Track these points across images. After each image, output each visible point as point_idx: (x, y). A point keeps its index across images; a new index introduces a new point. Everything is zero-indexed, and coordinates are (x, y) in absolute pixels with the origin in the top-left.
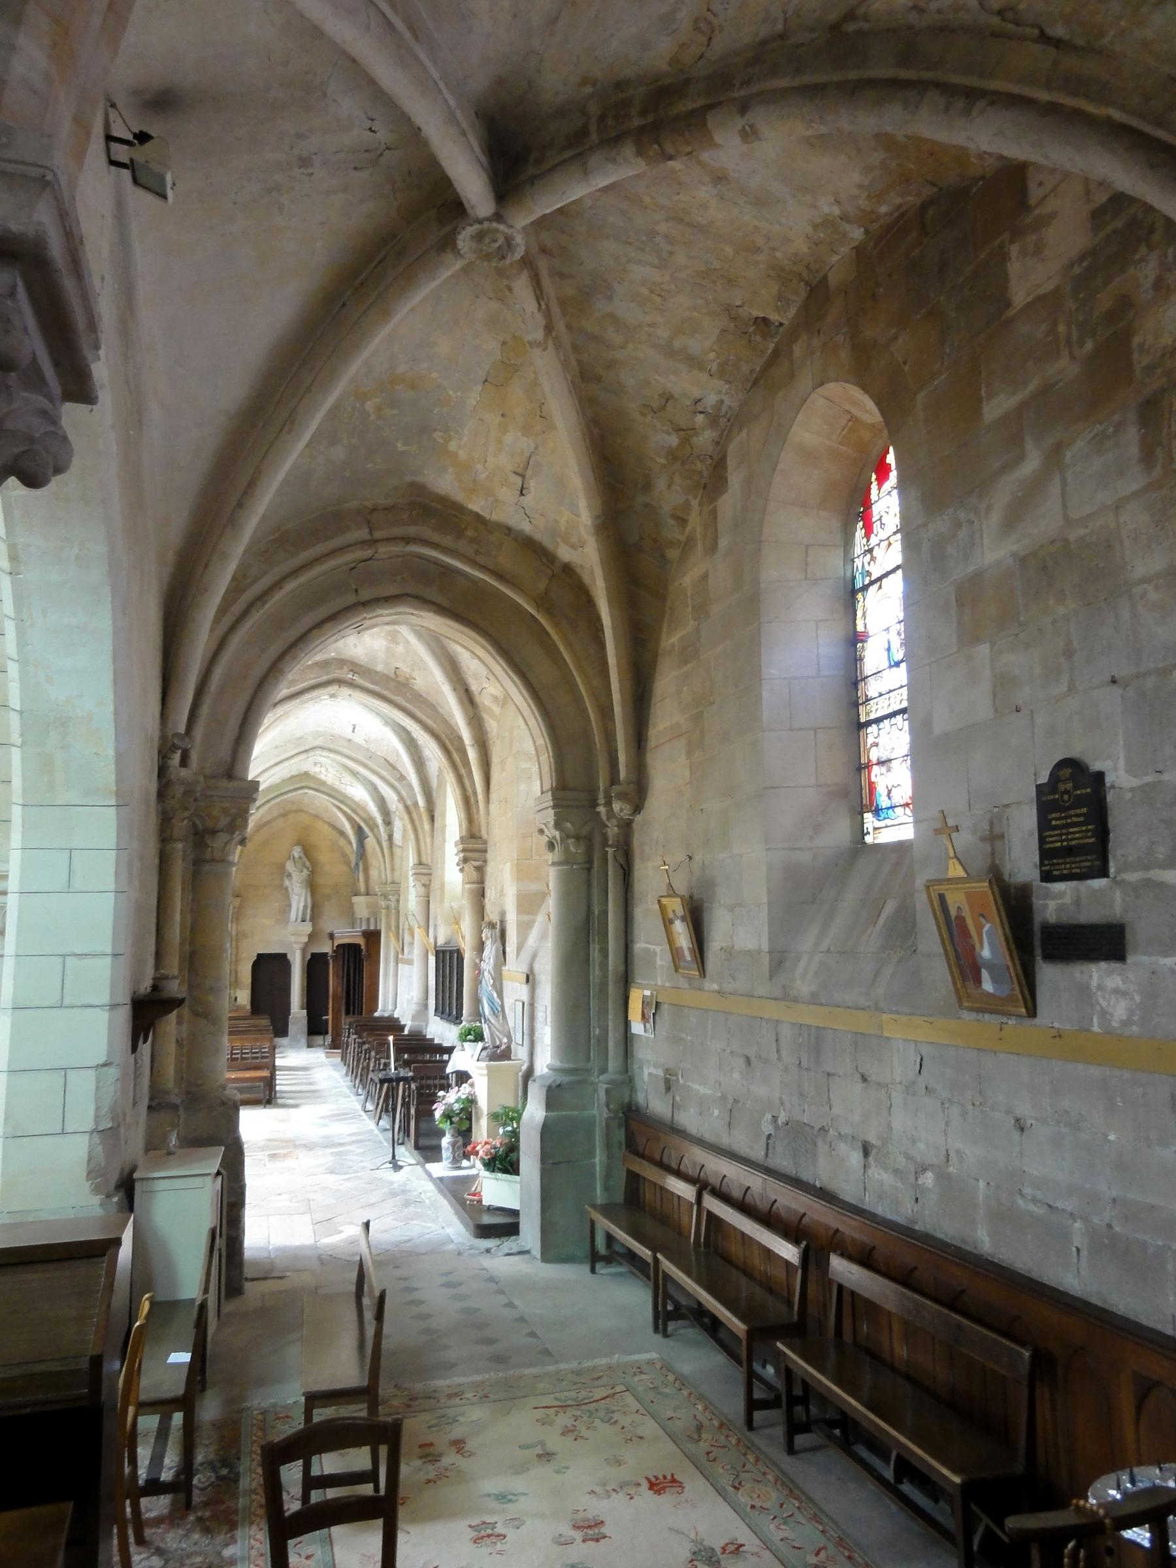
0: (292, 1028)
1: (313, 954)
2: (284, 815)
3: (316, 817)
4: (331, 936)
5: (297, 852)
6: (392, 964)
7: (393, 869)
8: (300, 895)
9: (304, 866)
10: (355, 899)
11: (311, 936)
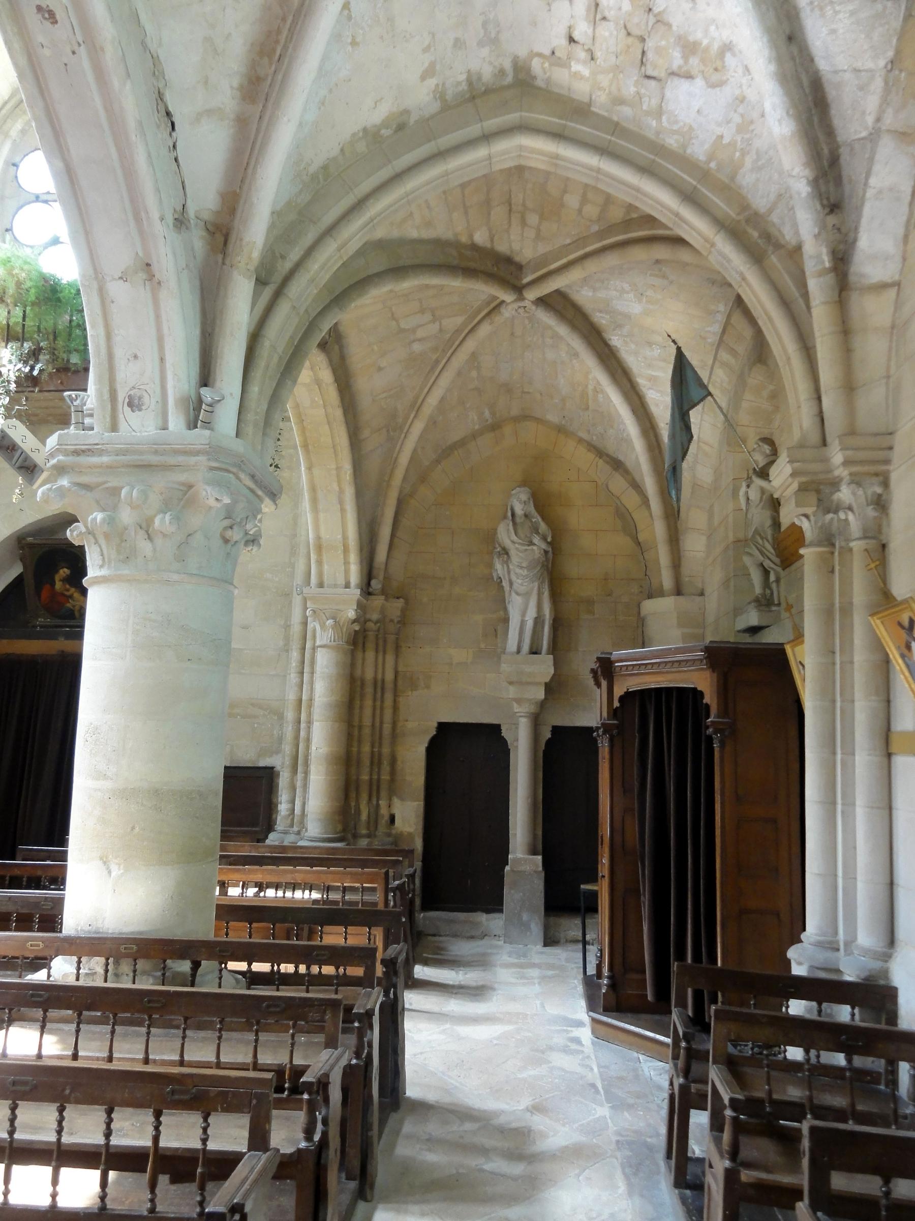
0: (511, 896)
1: (556, 730)
2: (495, 427)
3: (561, 430)
4: (606, 669)
5: (520, 503)
6: (863, 761)
7: (849, 387)
8: (527, 595)
9: (536, 530)
10: (649, 606)
11: (549, 688)
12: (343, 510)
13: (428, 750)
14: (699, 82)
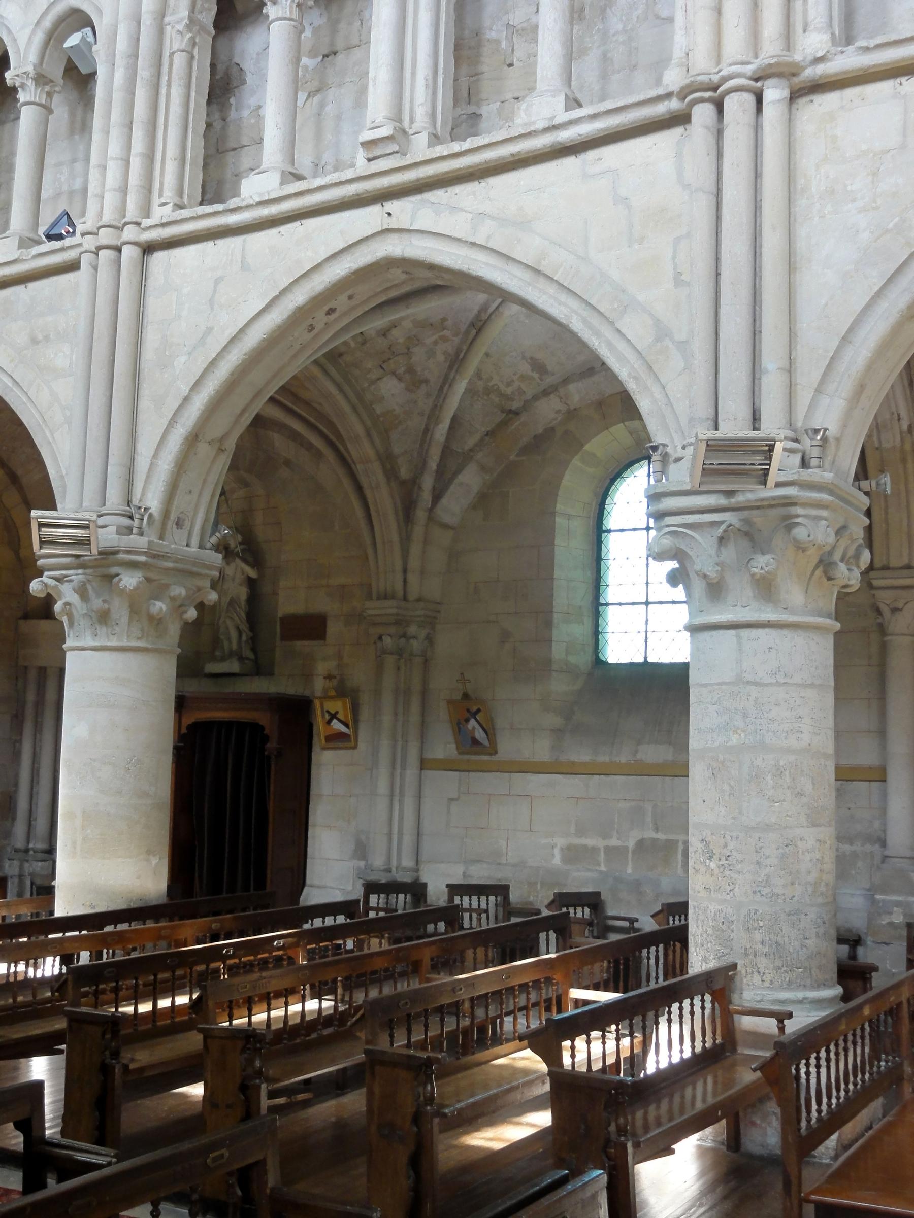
14: (403, 385)
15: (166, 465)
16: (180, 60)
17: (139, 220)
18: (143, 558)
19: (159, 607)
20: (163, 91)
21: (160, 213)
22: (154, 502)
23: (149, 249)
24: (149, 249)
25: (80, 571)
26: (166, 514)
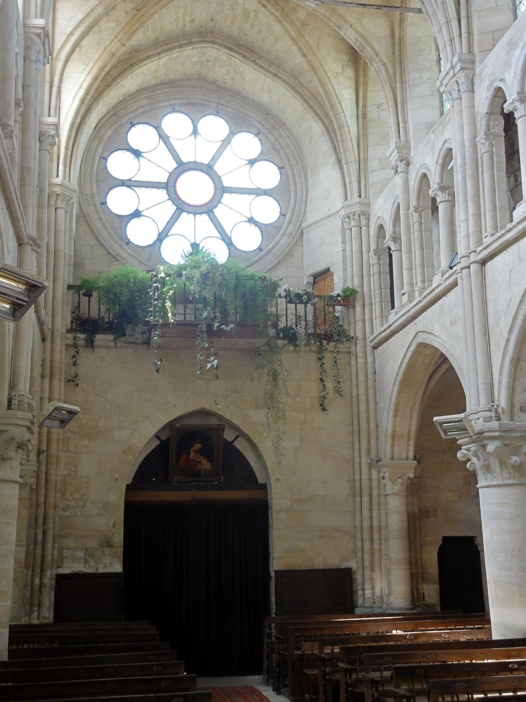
12: (411, 416)
13: (439, 553)
15: (505, 379)
16: (486, 157)
17: (475, 249)
18: (497, 434)
19: (515, 459)
20: (480, 177)
21: (486, 241)
22: (502, 401)
23: (483, 262)
24: (483, 262)
25: (474, 445)
26: (512, 406)
